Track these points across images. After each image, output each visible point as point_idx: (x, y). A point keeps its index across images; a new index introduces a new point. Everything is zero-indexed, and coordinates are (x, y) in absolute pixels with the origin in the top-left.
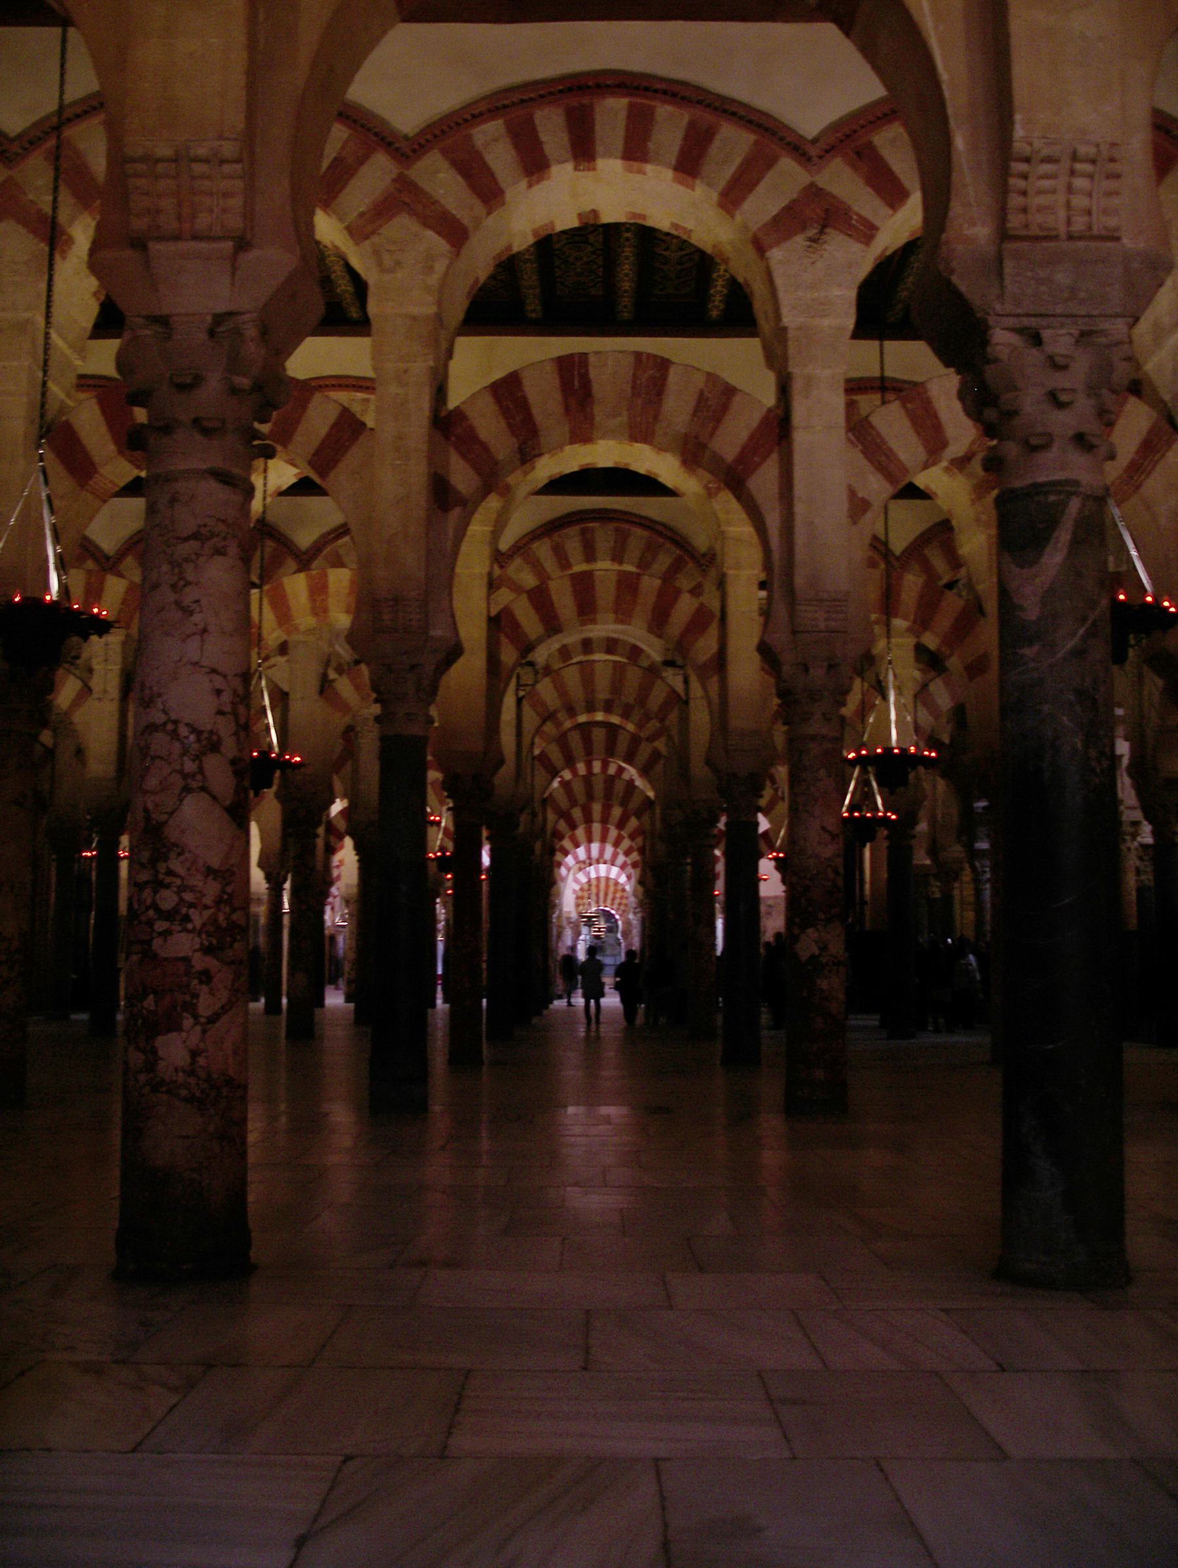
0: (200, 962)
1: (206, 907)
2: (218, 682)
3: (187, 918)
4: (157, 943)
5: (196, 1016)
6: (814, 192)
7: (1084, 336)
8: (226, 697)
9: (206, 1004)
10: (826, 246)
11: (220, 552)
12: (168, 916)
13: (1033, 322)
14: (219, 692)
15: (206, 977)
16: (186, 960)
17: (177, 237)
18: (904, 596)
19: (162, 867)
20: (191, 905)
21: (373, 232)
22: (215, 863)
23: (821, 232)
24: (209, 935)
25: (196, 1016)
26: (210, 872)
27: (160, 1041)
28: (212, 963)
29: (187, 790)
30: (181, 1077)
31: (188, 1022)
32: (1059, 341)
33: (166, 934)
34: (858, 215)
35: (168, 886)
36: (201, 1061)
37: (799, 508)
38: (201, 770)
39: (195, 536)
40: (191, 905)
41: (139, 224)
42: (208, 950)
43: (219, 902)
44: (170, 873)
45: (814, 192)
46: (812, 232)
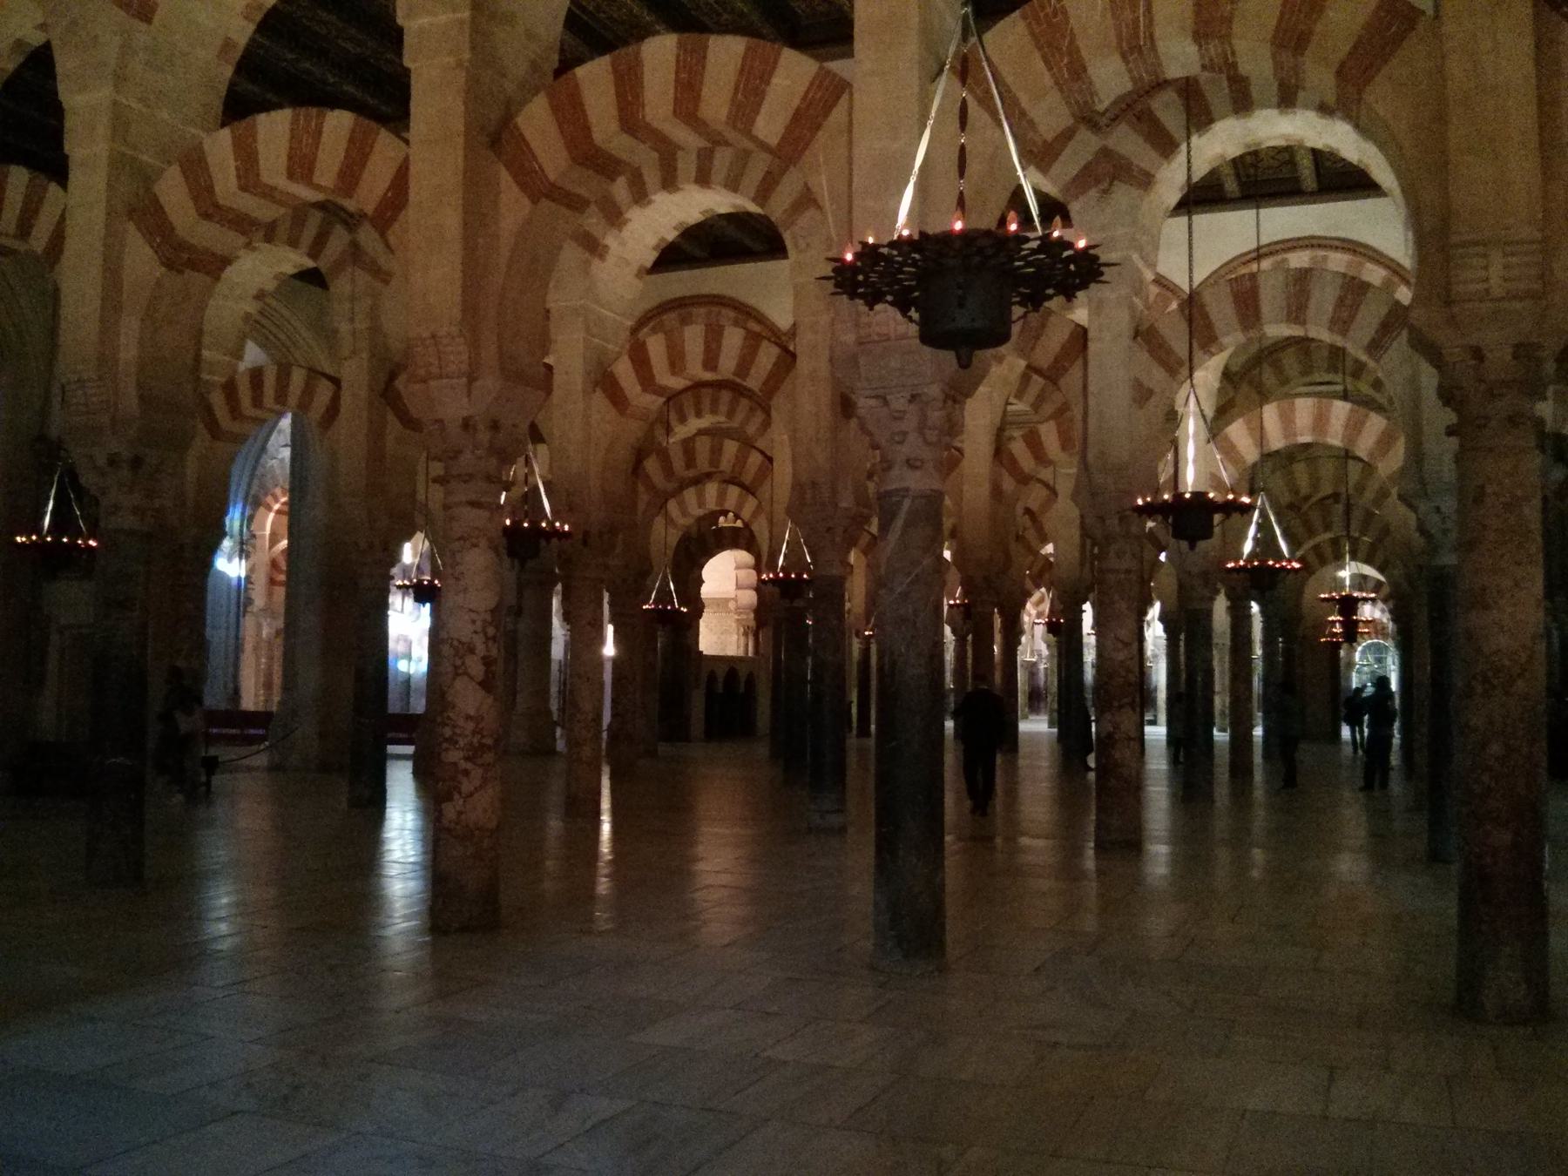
0: (463, 765)
1: (467, 736)
2: (474, 616)
3: (457, 742)
4: (443, 754)
5: (460, 793)
6: (1105, 153)
7: (913, 398)
8: (479, 623)
9: (466, 787)
10: (1113, 195)
11: (475, 546)
12: (446, 740)
13: (880, 392)
14: (474, 622)
15: (466, 773)
16: (455, 764)
17: (441, 377)
18: (1333, 421)
19: (445, 715)
20: (460, 735)
21: (792, 223)
22: (472, 713)
23: (1111, 184)
24: (468, 750)
25: (460, 793)
26: (468, 718)
27: (443, 806)
28: (469, 766)
29: (457, 674)
30: (453, 825)
31: (456, 796)
32: (899, 402)
33: (447, 750)
34: (1137, 166)
35: (447, 725)
36: (463, 817)
37: (1092, 402)
38: (463, 663)
39: (459, 539)
40: (460, 735)
41: (422, 372)
42: (467, 759)
43: (474, 733)
44: (449, 718)
45: (1105, 153)
46: (1105, 185)
